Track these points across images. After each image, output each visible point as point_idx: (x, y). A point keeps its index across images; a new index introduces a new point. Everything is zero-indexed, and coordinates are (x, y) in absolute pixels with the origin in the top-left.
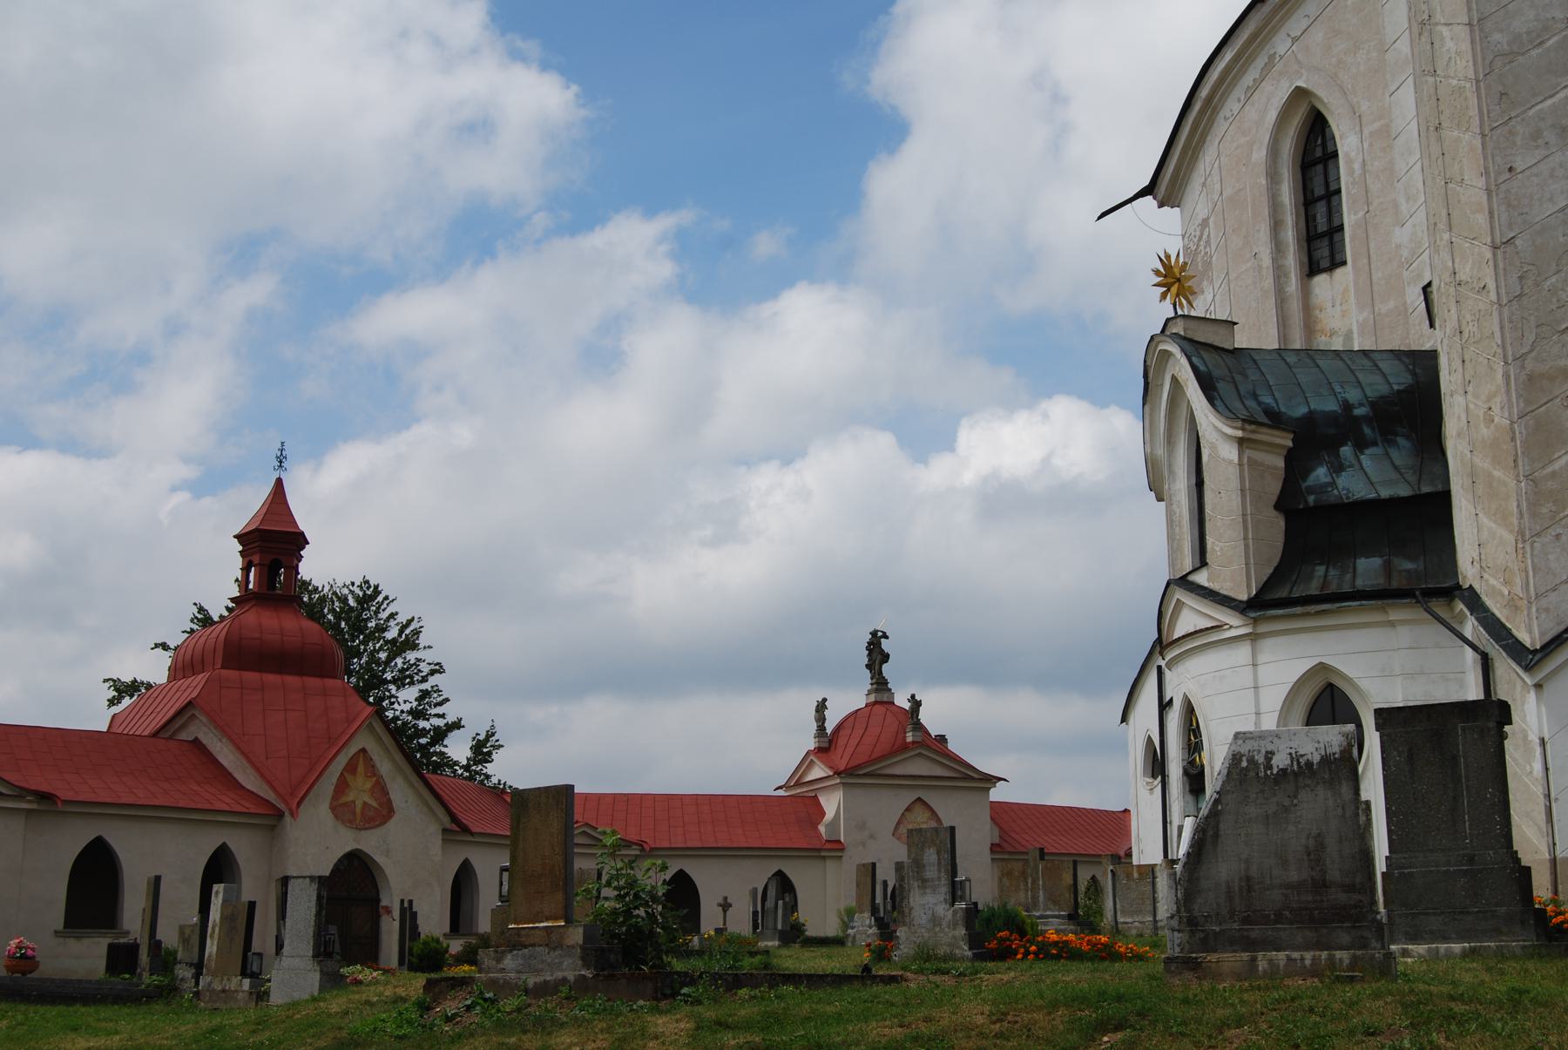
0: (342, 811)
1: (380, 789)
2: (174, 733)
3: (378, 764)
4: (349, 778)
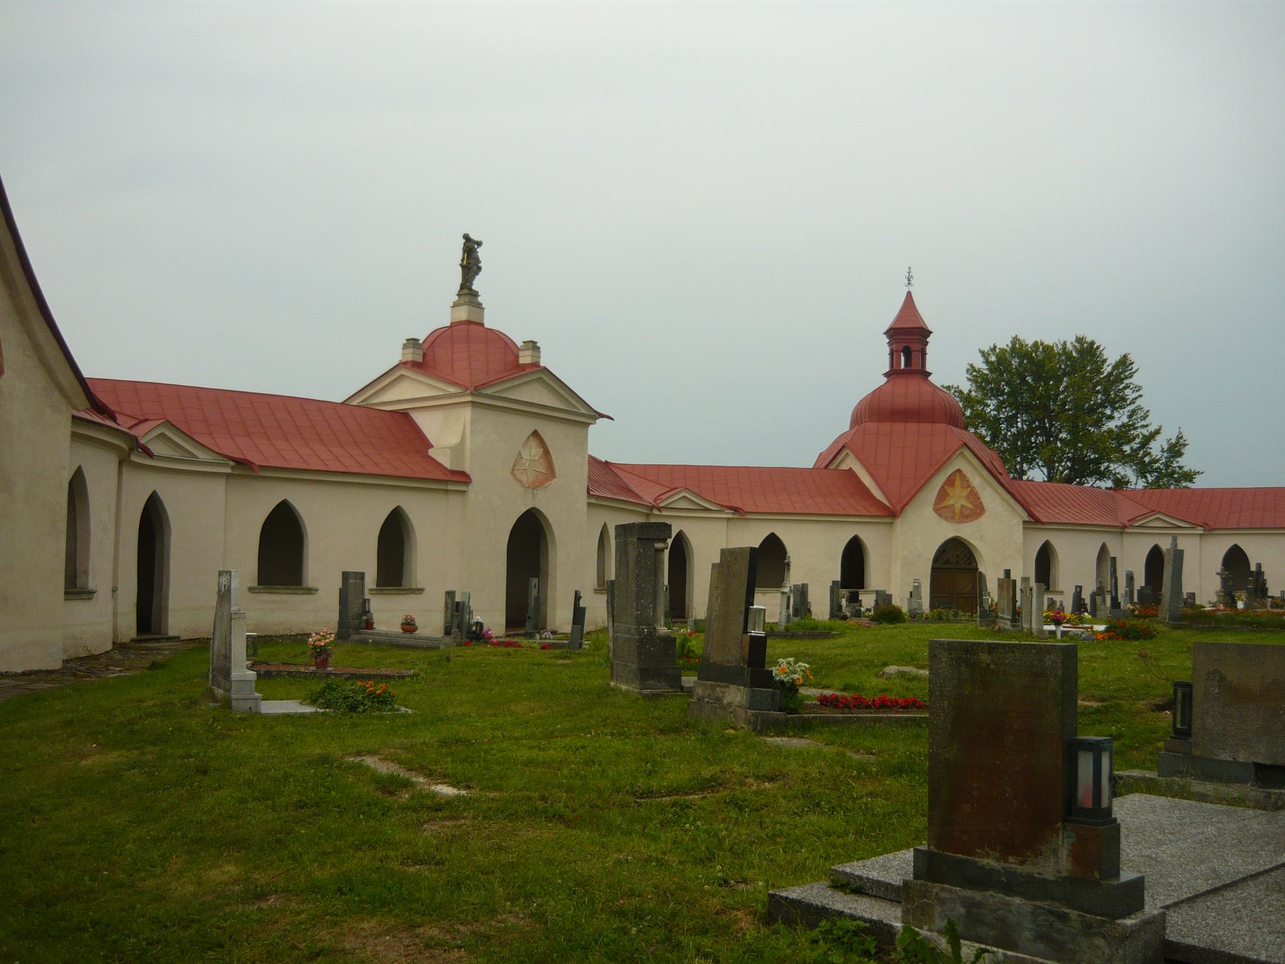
0: (942, 509)
1: (973, 496)
2: (838, 465)
3: (971, 480)
4: (949, 489)
